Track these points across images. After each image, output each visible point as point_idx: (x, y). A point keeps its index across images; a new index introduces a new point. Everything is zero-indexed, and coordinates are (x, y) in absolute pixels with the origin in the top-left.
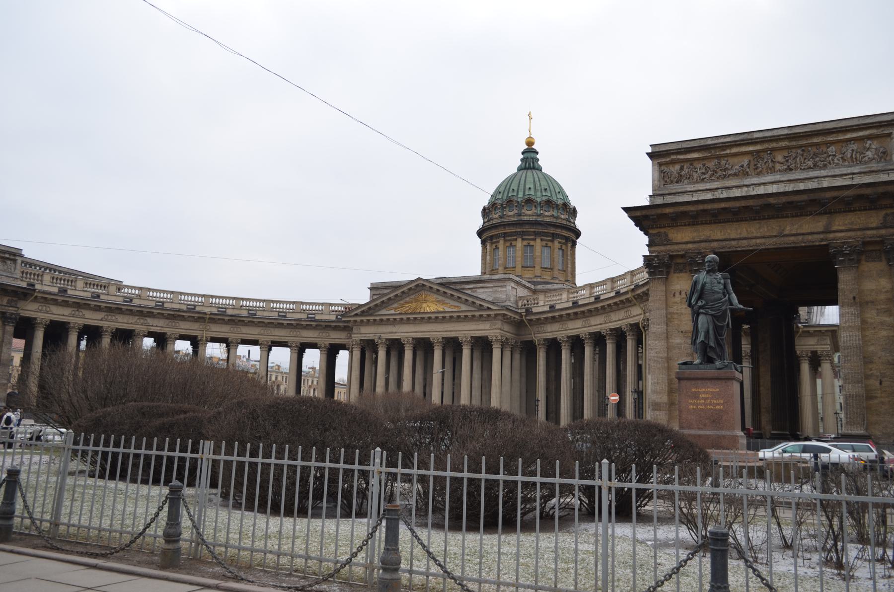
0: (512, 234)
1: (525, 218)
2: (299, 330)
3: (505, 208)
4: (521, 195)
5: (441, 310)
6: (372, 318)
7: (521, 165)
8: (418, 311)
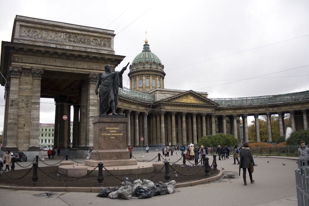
0: (154, 75)
4: (156, 61)
5: (195, 102)
8: (188, 102)
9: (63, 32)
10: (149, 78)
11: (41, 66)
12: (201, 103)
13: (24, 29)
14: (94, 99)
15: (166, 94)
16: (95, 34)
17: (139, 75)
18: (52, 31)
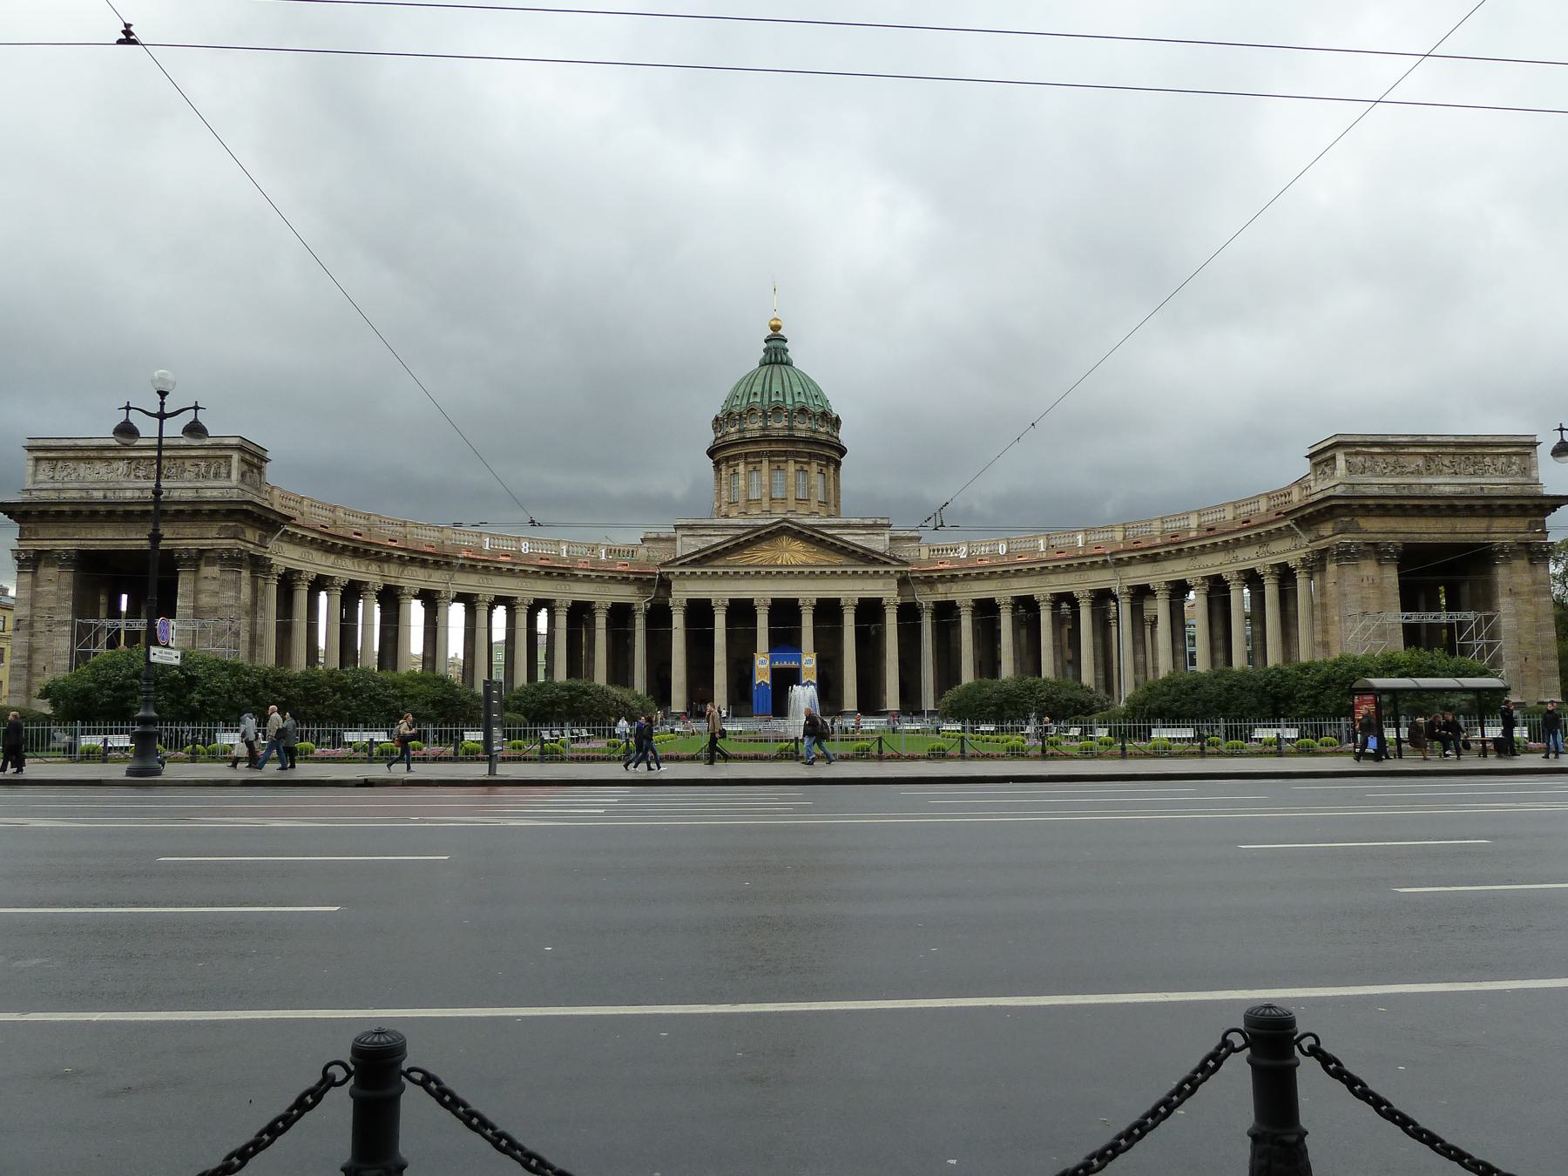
0: (779, 454)
1: (798, 434)
2: (570, 583)
3: (770, 417)
4: (789, 401)
5: (810, 561)
6: (709, 571)
7: (764, 359)
8: (779, 562)
9: (123, 459)
10: (758, 466)
11: (74, 542)
12: (837, 562)
13: (44, 465)
14: (186, 607)
15: (710, 535)
16: (193, 453)
17: (727, 459)
18: (100, 459)
